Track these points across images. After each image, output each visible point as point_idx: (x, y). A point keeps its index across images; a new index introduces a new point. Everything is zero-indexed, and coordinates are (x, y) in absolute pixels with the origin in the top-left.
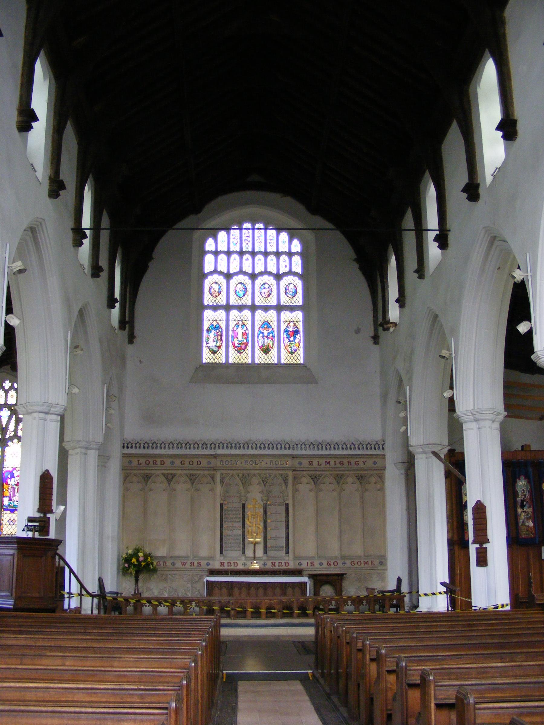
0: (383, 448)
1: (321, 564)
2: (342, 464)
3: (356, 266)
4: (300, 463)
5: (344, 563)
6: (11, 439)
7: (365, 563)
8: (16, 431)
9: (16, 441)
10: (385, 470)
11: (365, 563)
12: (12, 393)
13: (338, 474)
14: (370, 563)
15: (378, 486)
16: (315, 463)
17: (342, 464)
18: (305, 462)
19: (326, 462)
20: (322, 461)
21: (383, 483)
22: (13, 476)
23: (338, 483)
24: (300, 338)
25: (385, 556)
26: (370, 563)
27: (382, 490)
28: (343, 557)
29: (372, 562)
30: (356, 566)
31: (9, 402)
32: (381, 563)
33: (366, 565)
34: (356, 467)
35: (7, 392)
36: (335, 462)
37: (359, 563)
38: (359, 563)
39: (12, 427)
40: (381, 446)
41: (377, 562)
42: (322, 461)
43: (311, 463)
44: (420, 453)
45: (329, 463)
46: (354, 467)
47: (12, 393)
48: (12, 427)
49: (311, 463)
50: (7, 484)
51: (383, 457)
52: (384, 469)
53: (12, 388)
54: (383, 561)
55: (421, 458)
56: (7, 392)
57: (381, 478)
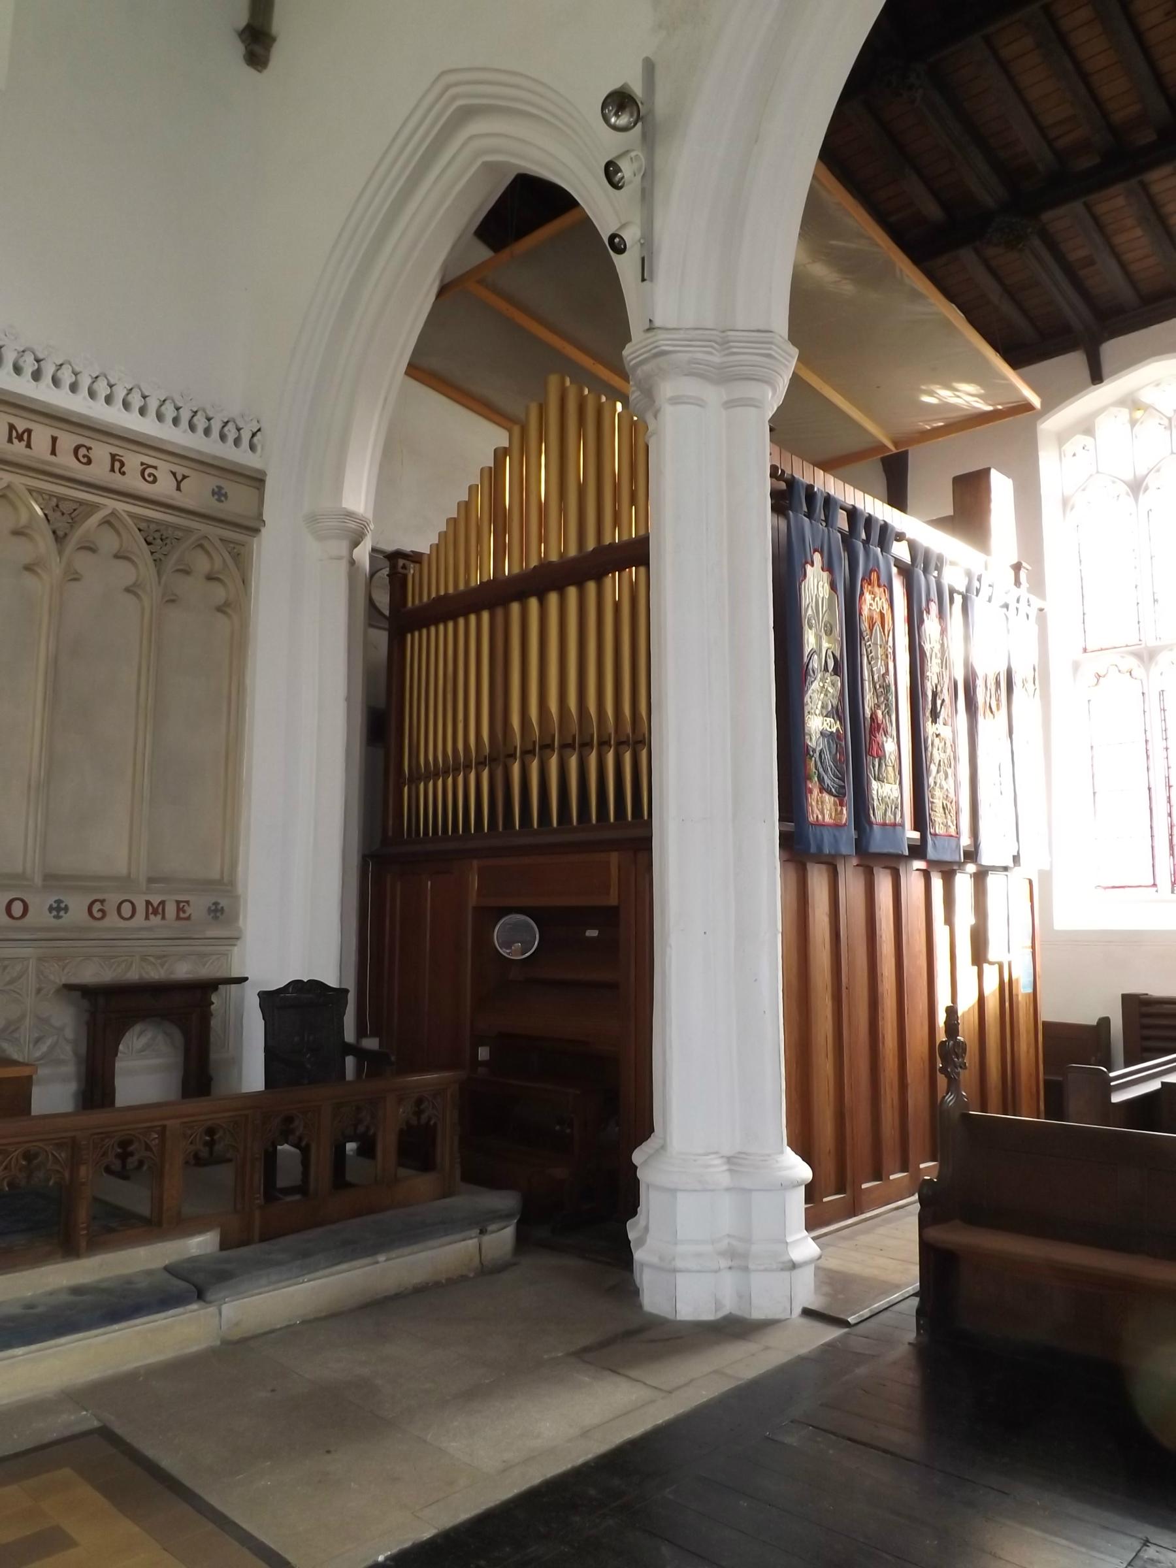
0: (252, 447)
5: (58, 909)
7: (153, 910)
10: (256, 531)
11: (153, 910)
13: (61, 499)
14: (171, 910)
15: (219, 594)
19: (12, 427)
21: (245, 582)
23: (59, 539)
25: (232, 883)
26: (171, 910)
27: (234, 608)
28: (52, 879)
29: (180, 907)
30: (112, 920)
32: (216, 912)
33: (155, 920)
36: (54, 440)
37: (126, 910)
38: (126, 910)
40: (246, 436)
41: (198, 905)
44: (695, 371)
45: (25, 437)
46: (133, 481)
51: (257, 481)
54: (223, 903)
55: (699, 403)
57: (240, 559)
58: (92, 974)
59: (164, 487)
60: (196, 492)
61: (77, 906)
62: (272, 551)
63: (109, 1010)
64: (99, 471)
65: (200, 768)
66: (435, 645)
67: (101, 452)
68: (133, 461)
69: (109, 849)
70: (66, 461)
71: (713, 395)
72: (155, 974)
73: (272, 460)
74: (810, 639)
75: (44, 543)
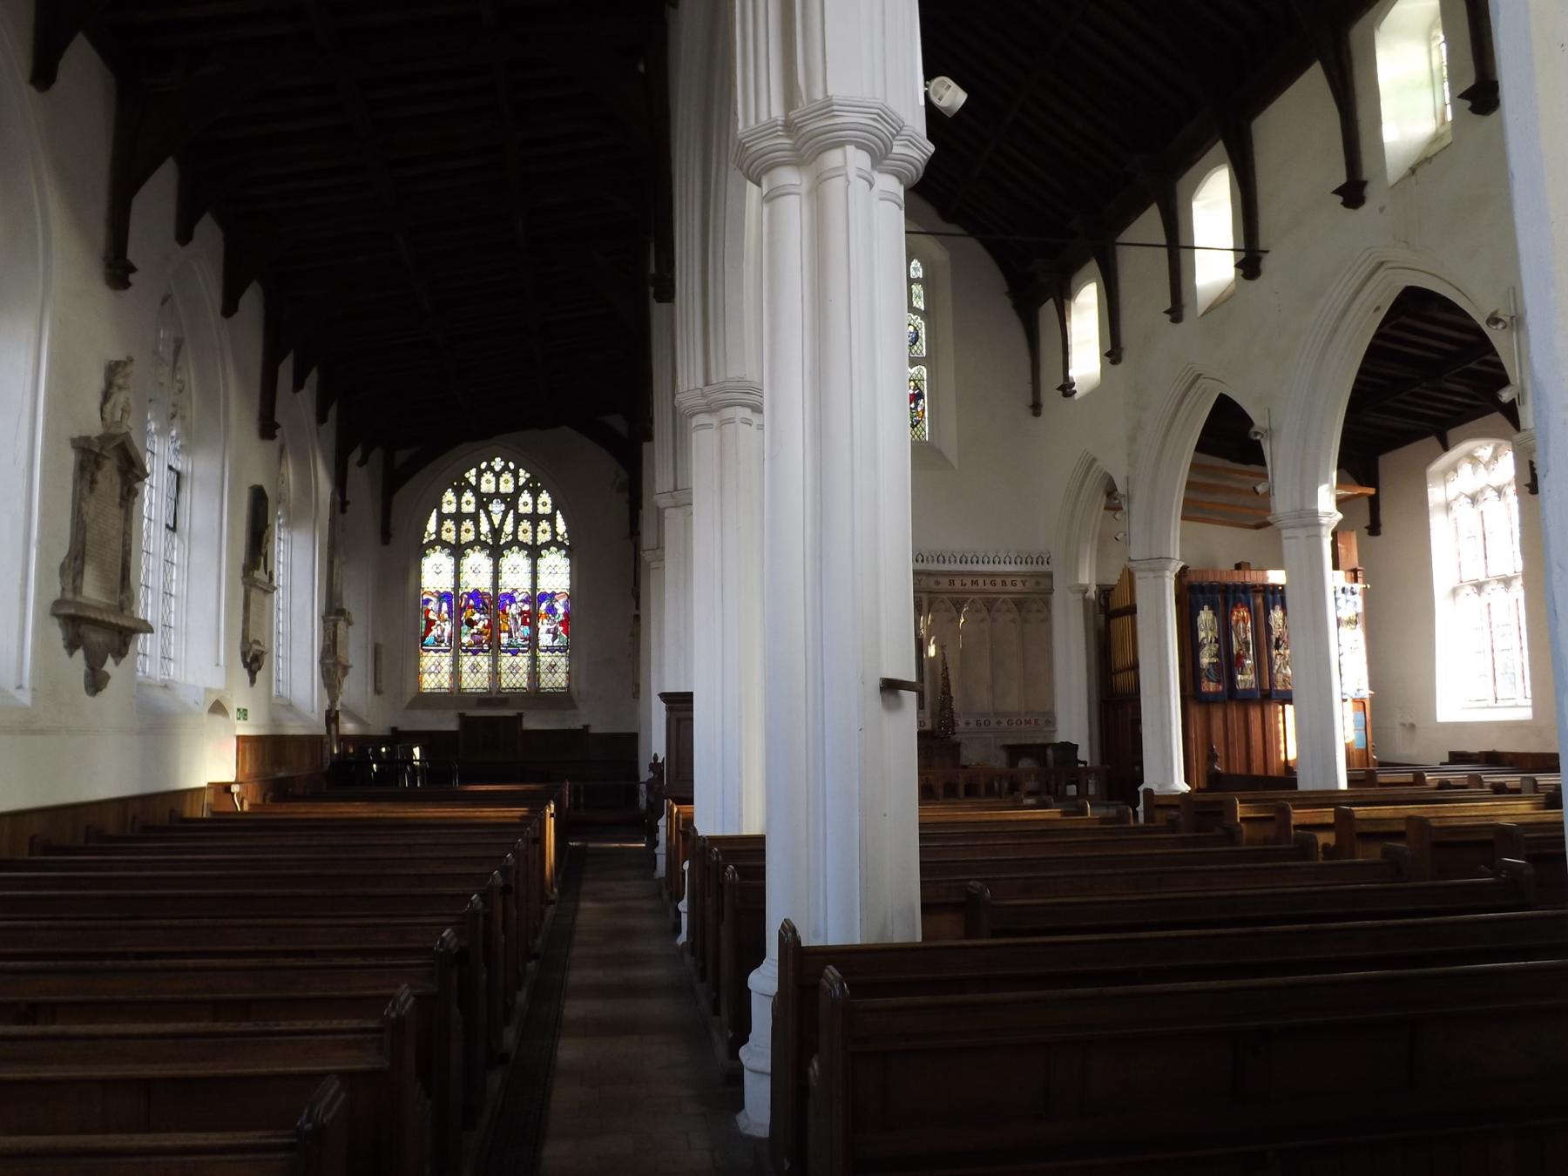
1: (967, 723)
2: (993, 583)
3: (1008, 302)
4: (937, 583)
5: (999, 723)
6: (509, 546)
8: (515, 533)
9: (515, 549)
12: (507, 476)
16: (958, 582)
17: (993, 583)
18: (944, 582)
20: (968, 581)
21: (1049, 611)
22: (513, 600)
24: (924, 403)
27: (1047, 620)
31: (502, 490)
34: (1012, 589)
35: (498, 475)
39: (508, 528)
42: (968, 581)
43: (952, 583)
45: (976, 583)
46: (1010, 588)
47: (507, 476)
48: (508, 528)
49: (952, 583)
50: (504, 612)
51: (1050, 575)
52: (1050, 591)
53: (505, 468)
56: (498, 475)
57: (1047, 604)
58: (1010, 742)
59: (1019, 586)
60: (1030, 584)
61: (1004, 722)
62: (1057, 599)
63: (1015, 752)
64: (999, 587)
65: (1039, 675)
66: (1117, 623)
67: (998, 581)
68: (1008, 581)
69: (1013, 703)
70: (989, 587)
71: (1151, 575)
72: (1030, 742)
73: (1056, 568)
74: (1202, 635)
75: (985, 613)
